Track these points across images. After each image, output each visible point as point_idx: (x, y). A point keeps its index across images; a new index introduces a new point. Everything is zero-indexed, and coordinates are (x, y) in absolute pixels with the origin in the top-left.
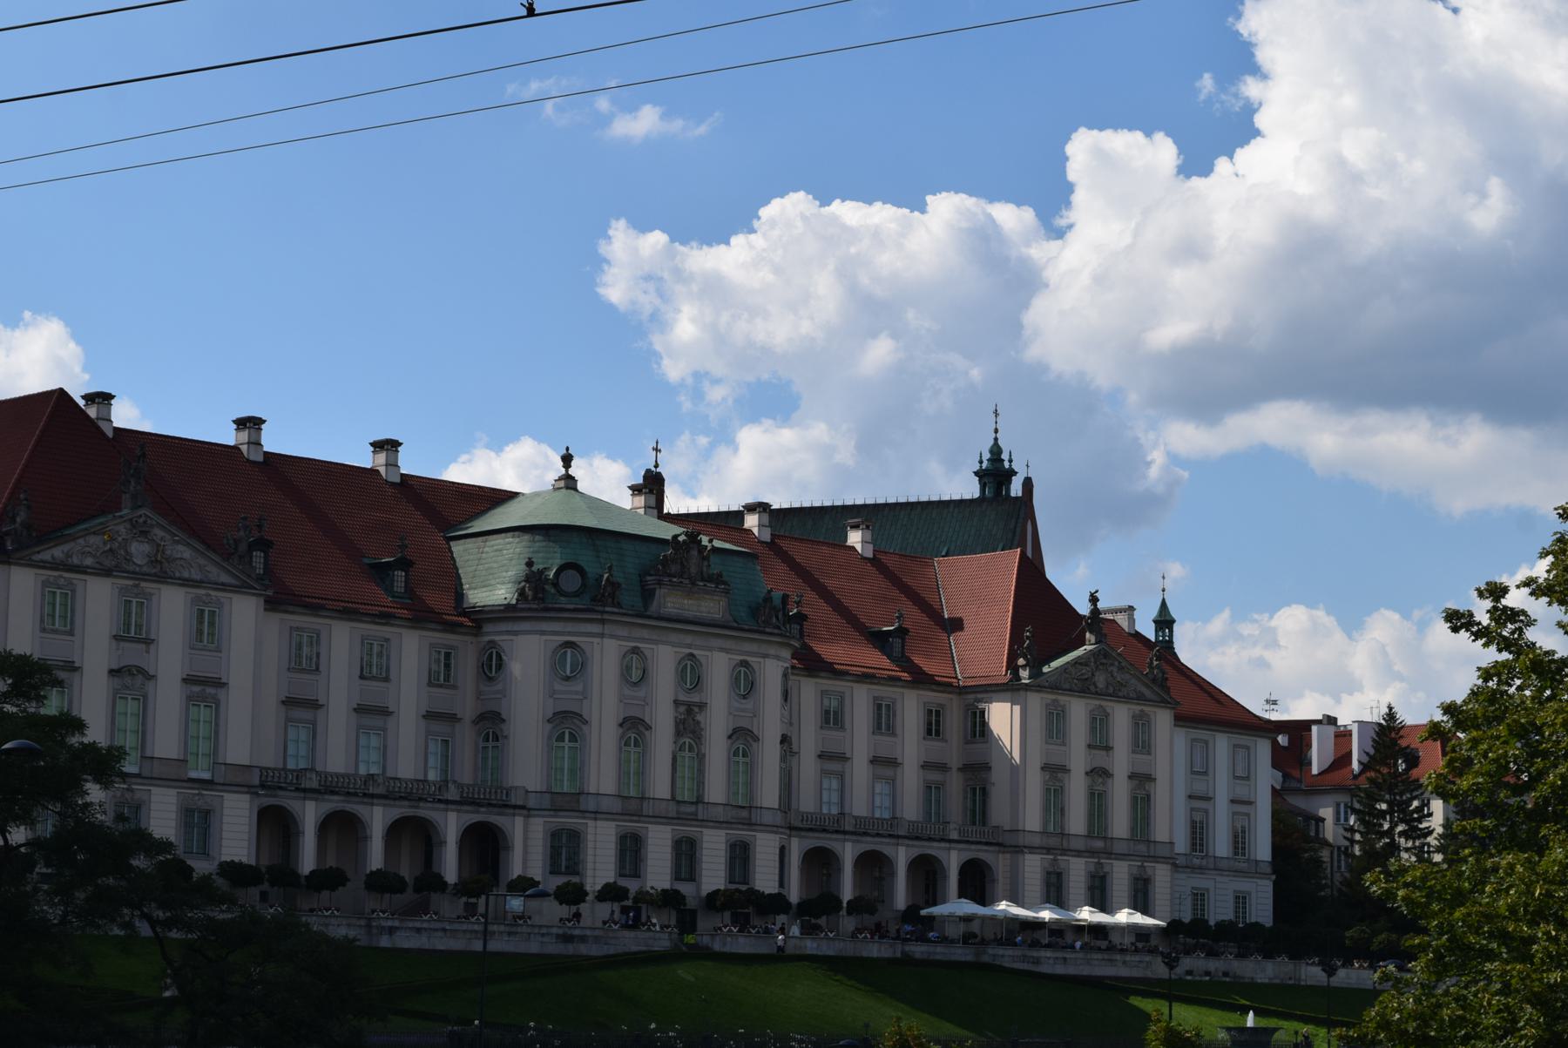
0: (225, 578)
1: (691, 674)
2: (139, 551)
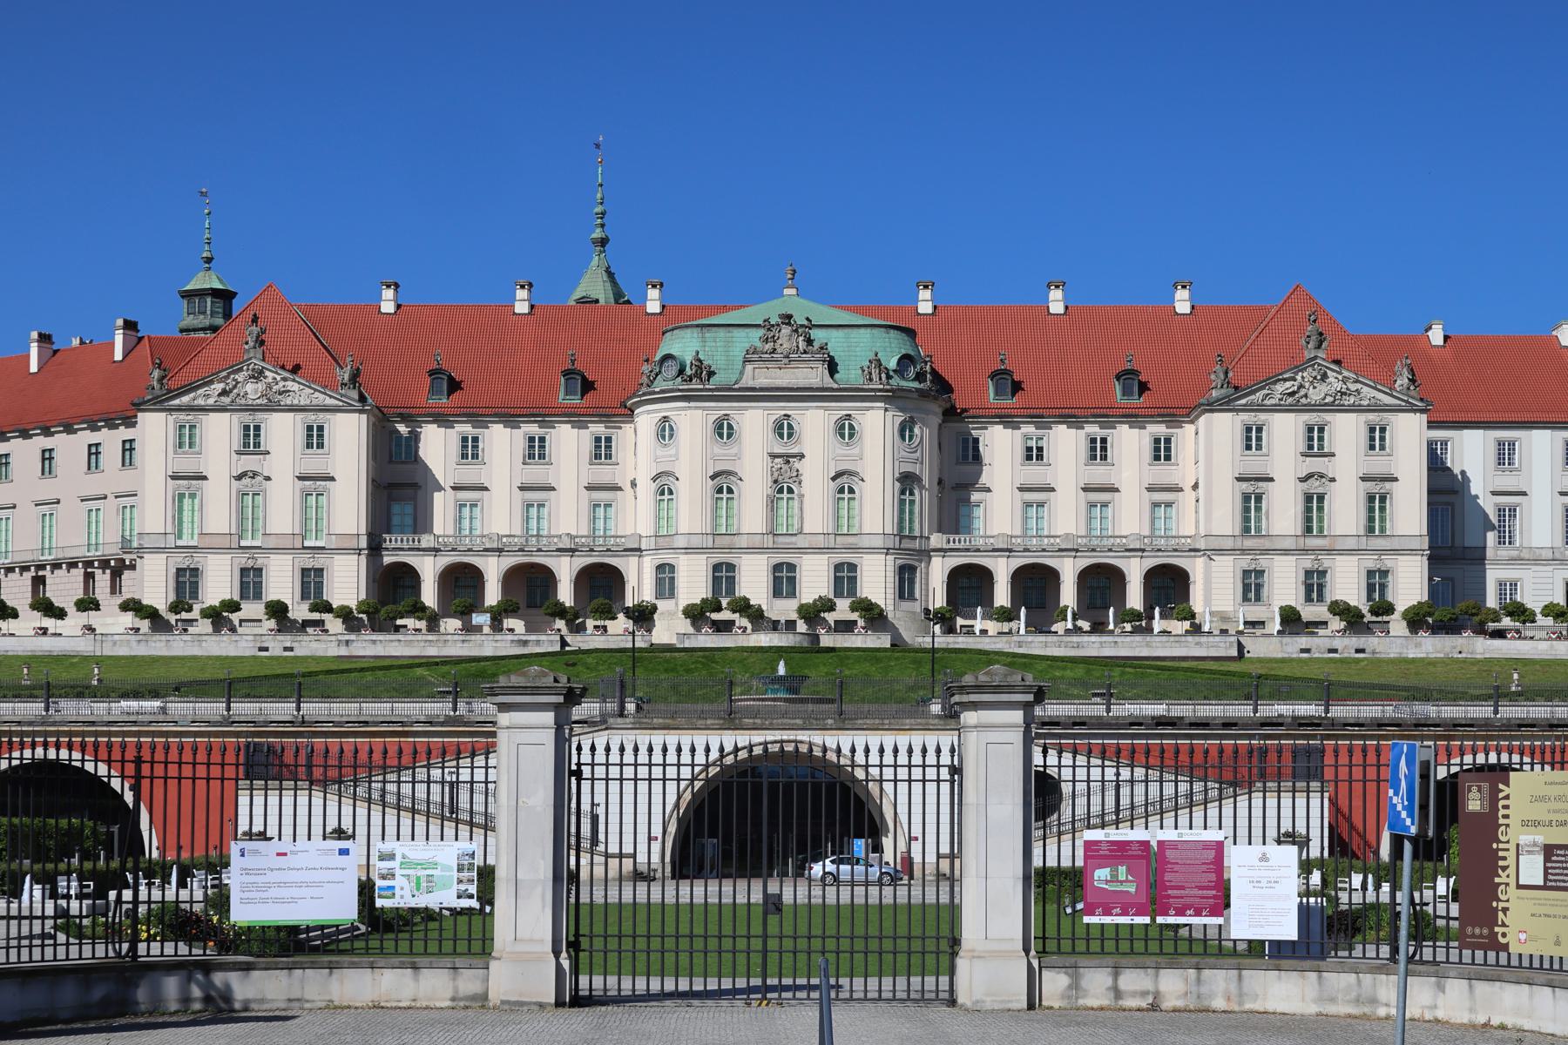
0: (329, 401)
1: (784, 429)
2: (252, 390)
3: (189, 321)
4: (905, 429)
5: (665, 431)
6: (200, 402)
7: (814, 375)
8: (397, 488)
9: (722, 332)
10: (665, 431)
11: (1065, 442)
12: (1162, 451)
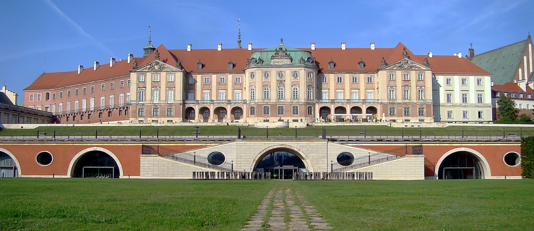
1: (280, 75)
3: (146, 55)
4: (308, 74)
5: (252, 76)
6: (145, 70)
7: (287, 61)
8: (188, 88)
9: (266, 53)
10: (252, 76)
11: (347, 78)
12: (369, 80)
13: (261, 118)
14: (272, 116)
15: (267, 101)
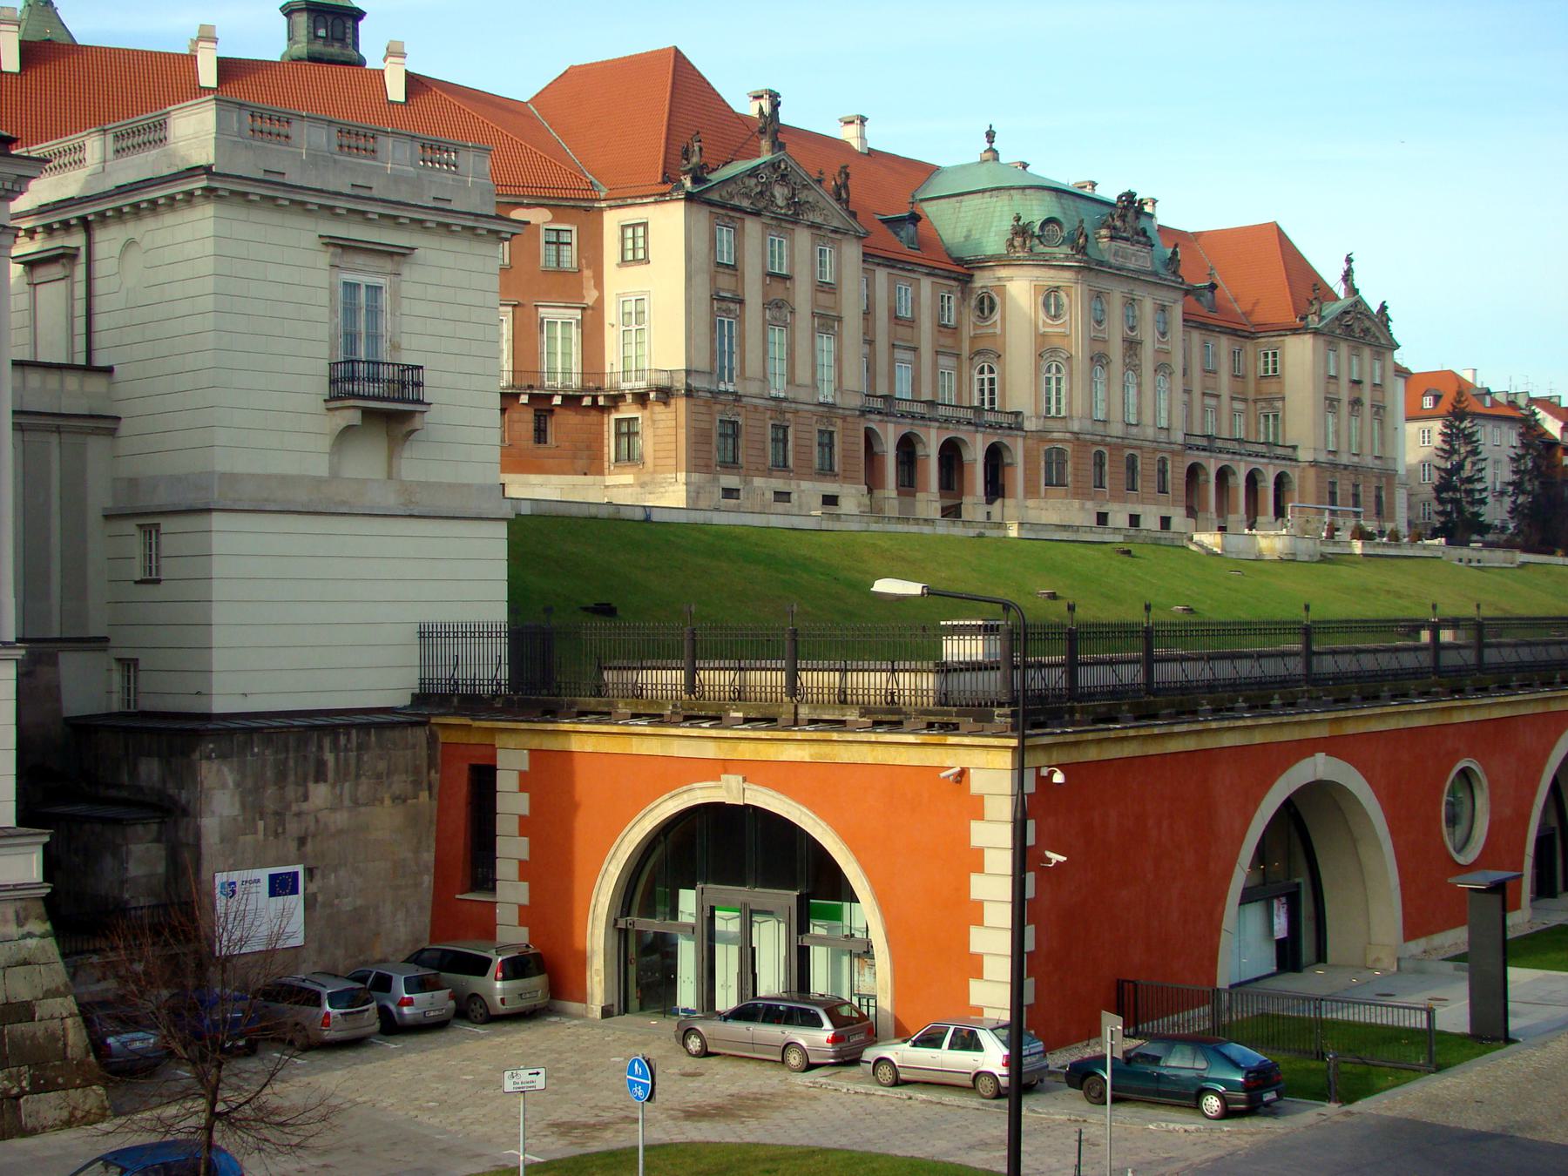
6: (736, 202)
13: (1089, 505)
14: (1116, 497)
15: (1099, 428)
